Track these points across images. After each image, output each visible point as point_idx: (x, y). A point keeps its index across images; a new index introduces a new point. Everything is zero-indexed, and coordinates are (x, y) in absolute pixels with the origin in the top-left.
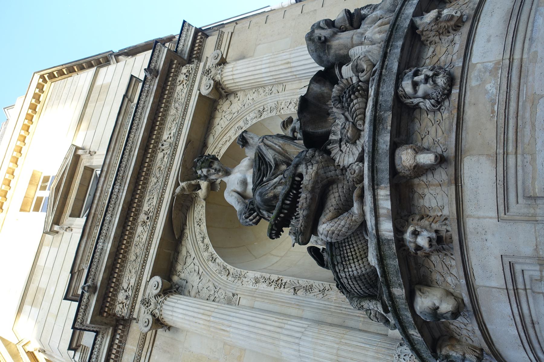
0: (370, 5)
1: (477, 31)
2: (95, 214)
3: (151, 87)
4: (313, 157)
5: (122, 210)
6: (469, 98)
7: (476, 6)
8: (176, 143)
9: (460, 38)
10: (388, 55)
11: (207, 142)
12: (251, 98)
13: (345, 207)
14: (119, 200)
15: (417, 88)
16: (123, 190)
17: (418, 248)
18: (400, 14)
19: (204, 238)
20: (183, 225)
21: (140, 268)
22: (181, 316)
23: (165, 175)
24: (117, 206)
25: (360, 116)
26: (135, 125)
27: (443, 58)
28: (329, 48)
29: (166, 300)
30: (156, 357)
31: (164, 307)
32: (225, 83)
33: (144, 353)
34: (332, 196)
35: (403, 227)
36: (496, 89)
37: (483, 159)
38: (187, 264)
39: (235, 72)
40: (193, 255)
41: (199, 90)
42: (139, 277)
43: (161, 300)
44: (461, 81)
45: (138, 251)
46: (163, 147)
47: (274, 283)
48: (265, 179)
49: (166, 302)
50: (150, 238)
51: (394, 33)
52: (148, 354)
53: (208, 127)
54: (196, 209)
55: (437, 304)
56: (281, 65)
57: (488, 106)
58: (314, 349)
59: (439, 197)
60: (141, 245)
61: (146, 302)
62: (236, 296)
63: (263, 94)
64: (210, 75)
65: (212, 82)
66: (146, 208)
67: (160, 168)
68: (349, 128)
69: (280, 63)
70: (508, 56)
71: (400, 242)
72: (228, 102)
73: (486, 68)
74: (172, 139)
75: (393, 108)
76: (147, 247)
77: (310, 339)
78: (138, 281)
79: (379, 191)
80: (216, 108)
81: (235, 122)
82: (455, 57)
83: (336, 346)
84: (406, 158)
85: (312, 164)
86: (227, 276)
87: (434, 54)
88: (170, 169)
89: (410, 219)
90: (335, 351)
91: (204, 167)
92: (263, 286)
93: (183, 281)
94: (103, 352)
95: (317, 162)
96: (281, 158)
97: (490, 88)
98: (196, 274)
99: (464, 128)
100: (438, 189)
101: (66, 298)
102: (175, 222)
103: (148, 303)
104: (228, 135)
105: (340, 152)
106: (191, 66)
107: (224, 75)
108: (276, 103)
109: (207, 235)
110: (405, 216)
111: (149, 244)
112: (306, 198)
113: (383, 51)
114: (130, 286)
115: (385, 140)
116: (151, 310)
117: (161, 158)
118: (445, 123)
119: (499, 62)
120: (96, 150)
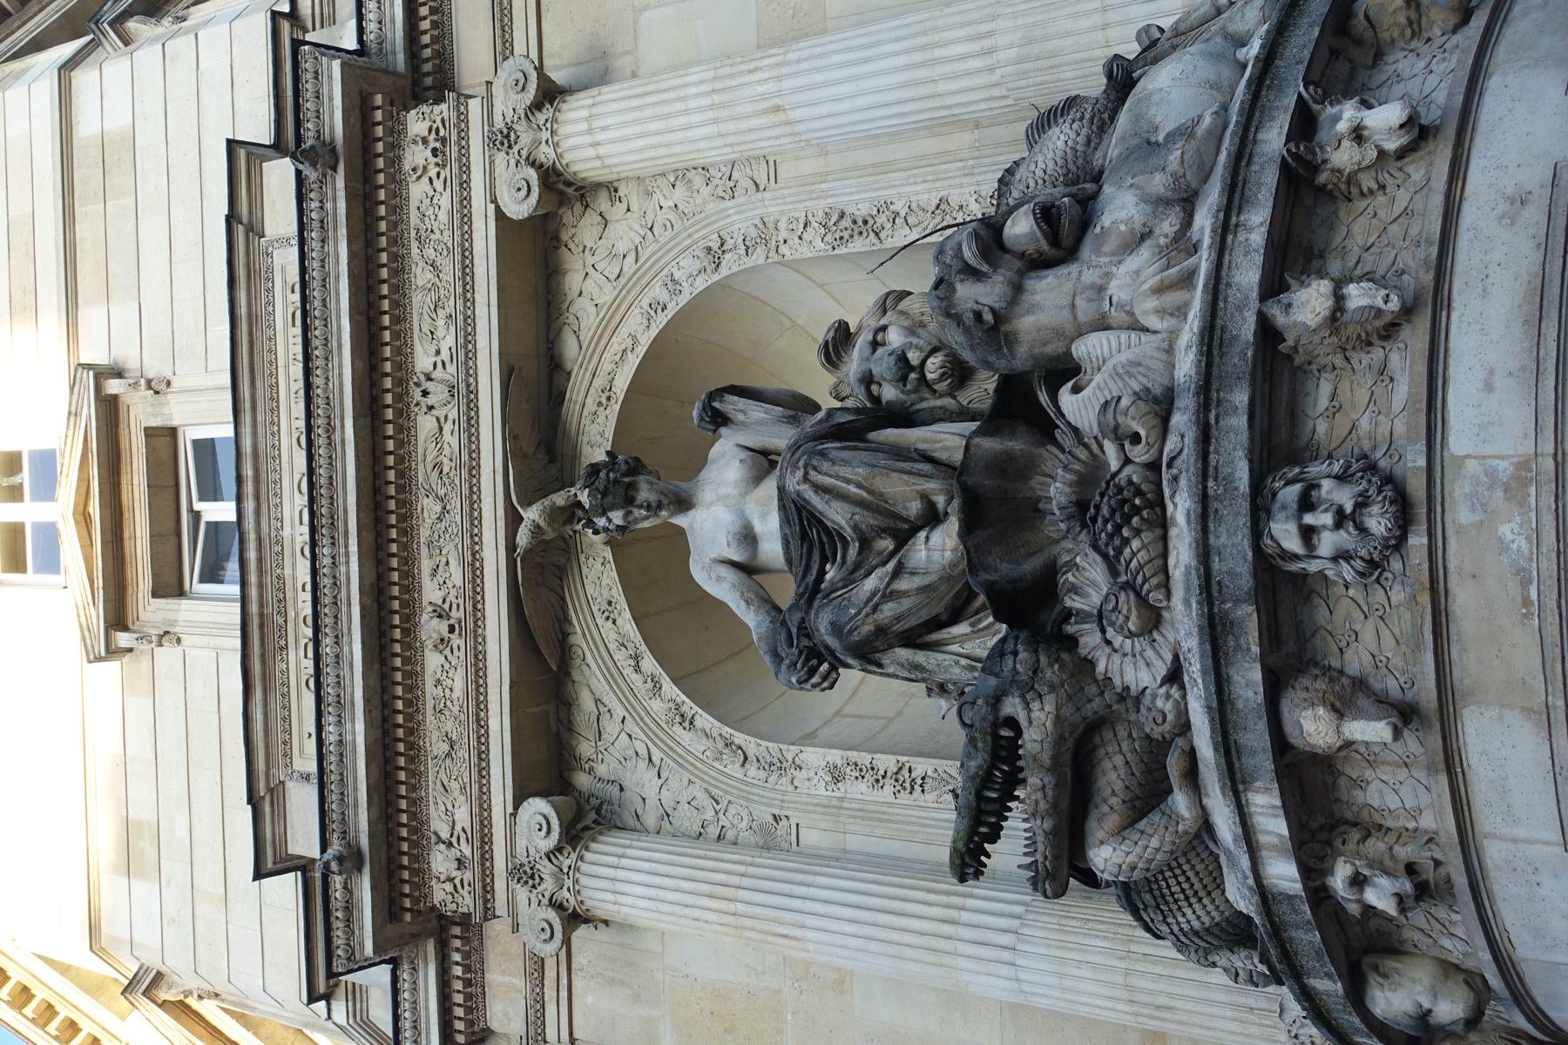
0: (1072, 102)
1: (1451, 345)
2: (261, 615)
3: (329, 205)
4: (1035, 672)
5: (363, 617)
6: (1457, 556)
7: (1434, 251)
8: (468, 385)
9: (1405, 360)
10: (1214, 432)
11: (561, 355)
12: (667, 204)
13: (1149, 796)
14: (344, 590)
15: (1315, 541)
16: (347, 554)
17: (1369, 910)
18: (1222, 287)
19: (637, 658)
20: (560, 621)
21: (475, 776)
22: (644, 903)
23: (466, 491)
24: (344, 608)
25: (1154, 581)
26: (315, 343)
27: (1365, 424)
28: (1010, 340)
29: (581, 858)
30: (590, 999)
31: (584, 880)
32: (574, 168)
33: (550, 992)
34: (1107, 765)
35: (1322, 859)
36: (1528, 539)
37: (1514, 717)
38: (608, 737)
39: (600, 137)
40: (619, 712)
41: (494, 201)
42: (475, 803)
43: (568, 862)
44: (1430, 510)
45: (450, 725)
46: (431, 400)
47: (889, 782)
48: (831, 573)
49: (584, 867)
50: (478, 686)
51: (1216, 359)
52: (564, 994)
53: (549, 305)
54: (585, 571)
55: (1426, 1005)
56: (757, 114)
57: (1513, 585)
58: (1061, 975)
59: (1405, 791)
60: (456, 709)
61: (525, 874)
62: (784, 822)
63: (706, 191)
64: (516, 149)
65: (532, 174)
66: (431, 592)
67: (438, 466)
68: (1129, 610)
69: (749, 108)
70: (1549, 447)
71: (1319, 895)
72: (591, 218)
73: (1491, 474)
74: (451, 369)
75: (1256, 594)
76: (478, 715)
77: (1042, 951)
78: (481, 815)
79: (1250, 795)
80: (558, 239)
81: (638, 288)
82: (1400, 428)
83: (1118, 963)
85: (1040, 696)
86: (743, 765)
87: (1336, 410)
88: (474, 470)
89: (1338, 842)
90: (1120, 979)
91: (613, 507)
92: (857, 789)
93: (610, 788)
94: (427, 1008)
95: (1052, 688)
96: (868, 520)
97: (1509, 537)
98: (643, 764)
99: (1454, 637)
100: (1403, 774)
101: (259, 874)
102: (538, 626)
103: (532, 877)
104: (624, 330)
105: (1108, 650)
106: (437, 109)
107: (565, 145)
108: (757, 221)
109: (644, 648)
110: (1321, 828)
111: (481, 705)
112: (1043, 788)
113: (1198, 422)
114: (458, 828)
115: (1248, 679)
116: (547, 895)
117: (432, 433)
118: (1400, 618)
119: (1527, 462)
120: (168, 374)
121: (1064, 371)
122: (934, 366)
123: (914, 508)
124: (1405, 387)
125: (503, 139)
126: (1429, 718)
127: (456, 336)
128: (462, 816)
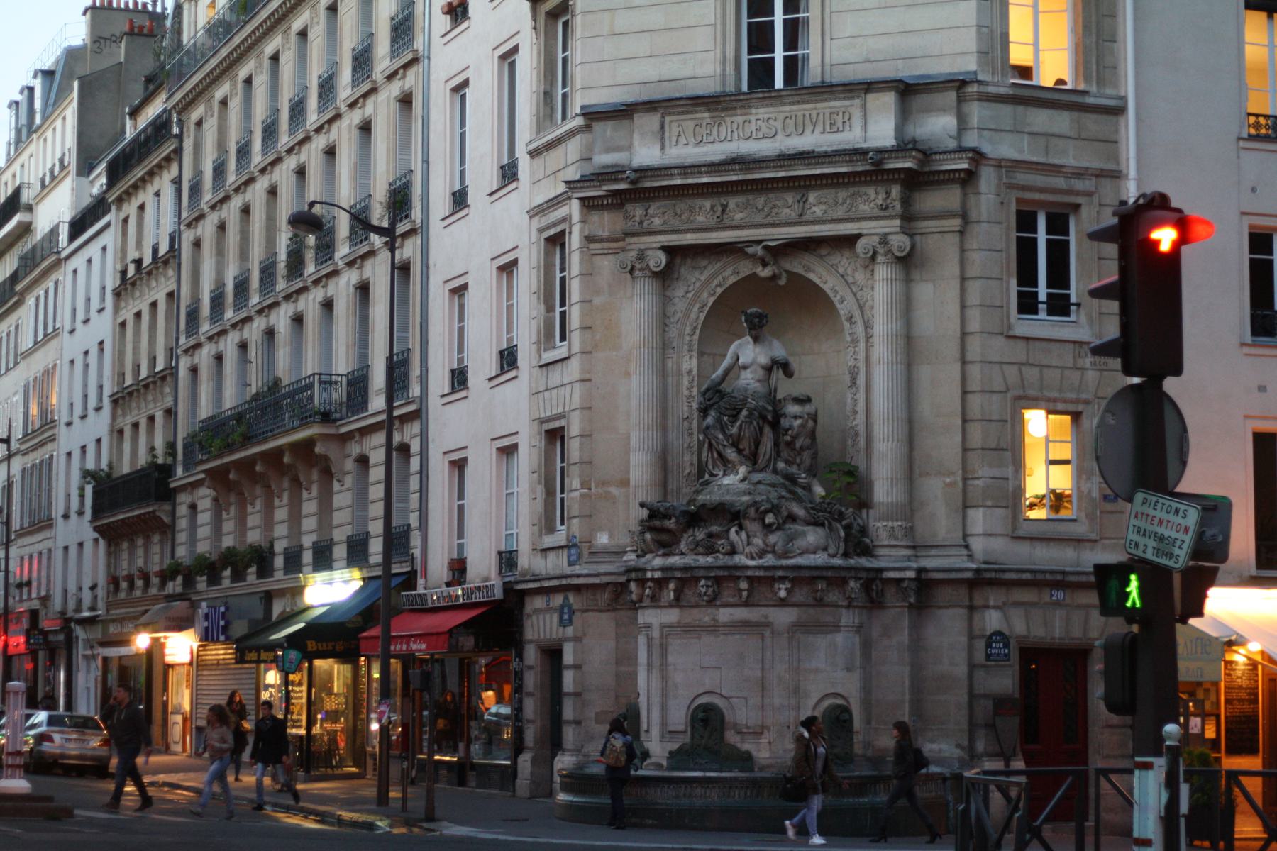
13: (662, 545)
19: (720, 285)
33: (606, 245)
48: (726, 418)
67: (775, 206)
71: (648, 580)
88: (773, 225)
92: (686, 382)
115: (678, 574)
117: (787, 205)
121: (741, 527)
122: (788, 438)
124: (731, 600)
125: (884, 239)
126: (677, 602)
127: (822, 215)
128: (657, 221)
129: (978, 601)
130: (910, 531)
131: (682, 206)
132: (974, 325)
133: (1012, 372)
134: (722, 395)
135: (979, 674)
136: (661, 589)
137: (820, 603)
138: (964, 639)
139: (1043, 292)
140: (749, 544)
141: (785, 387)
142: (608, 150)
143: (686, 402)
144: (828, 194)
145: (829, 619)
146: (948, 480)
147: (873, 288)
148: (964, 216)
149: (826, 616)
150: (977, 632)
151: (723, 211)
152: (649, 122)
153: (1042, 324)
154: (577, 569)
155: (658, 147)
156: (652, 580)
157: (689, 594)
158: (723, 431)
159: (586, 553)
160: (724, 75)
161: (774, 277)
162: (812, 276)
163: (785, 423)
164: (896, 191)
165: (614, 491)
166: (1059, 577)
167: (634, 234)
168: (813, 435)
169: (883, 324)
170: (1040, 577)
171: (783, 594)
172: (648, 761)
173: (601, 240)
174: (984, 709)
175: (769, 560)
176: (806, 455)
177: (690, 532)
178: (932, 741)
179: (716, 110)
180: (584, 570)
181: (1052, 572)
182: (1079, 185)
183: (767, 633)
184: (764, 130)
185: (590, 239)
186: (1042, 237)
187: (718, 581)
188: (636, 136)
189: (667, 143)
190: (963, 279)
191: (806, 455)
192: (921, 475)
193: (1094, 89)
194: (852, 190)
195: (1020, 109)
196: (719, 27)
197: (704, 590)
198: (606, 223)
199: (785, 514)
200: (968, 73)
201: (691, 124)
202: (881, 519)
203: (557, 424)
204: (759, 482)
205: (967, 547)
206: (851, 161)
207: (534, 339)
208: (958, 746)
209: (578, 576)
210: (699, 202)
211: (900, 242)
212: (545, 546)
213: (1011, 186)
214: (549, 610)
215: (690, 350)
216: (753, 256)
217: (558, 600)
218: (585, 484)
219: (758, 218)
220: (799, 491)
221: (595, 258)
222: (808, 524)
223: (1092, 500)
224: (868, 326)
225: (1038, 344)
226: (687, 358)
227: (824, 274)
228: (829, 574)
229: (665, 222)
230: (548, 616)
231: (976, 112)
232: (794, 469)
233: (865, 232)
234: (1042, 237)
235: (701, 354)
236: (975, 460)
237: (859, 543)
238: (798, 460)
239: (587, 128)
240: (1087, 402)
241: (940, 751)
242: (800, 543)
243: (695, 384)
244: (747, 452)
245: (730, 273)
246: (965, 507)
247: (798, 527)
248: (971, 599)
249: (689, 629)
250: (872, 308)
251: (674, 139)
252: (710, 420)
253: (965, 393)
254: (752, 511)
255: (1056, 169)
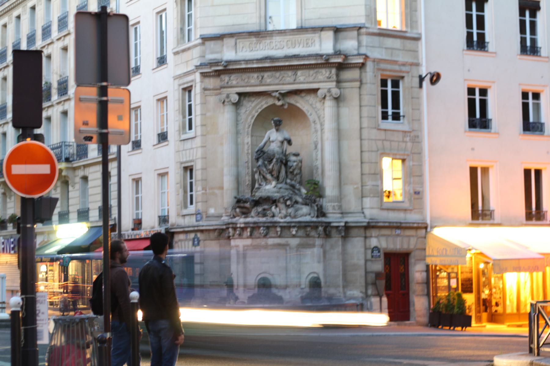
19: (260, 108)
33: (212, 91)
45: (246, 80)
71: (237, 228)
84: (249, 230)
88: (283, 84)
92: (246, 147)
115: (251, 225)
117: (289, 76)
121: (277, 206)
122: (291, 170)
123: (273, 173)
124: (273, 235)
125: (329, 91)
126: (251, 236)
128: (234, 83)
129: (368, 234)
130: (340, 207)
131: (245, 76)
132: (365, 125)
133: (379, 143)
134: (264, 153)
135: (369, 264)
136: (243, 231)
137: (308, 236)
138: (363, 250)
139: (390, 111)
140: (280, 213)
141: (290, 150)
142: (212, 53)
143: (247, 156)
144: (306, 72)
145: (311, 242)
146: (355, 186)
147: (324, 109)
148: (361, 81)
149: (310, 241)
150: (368, 247)
151: (262, 78)
152: (230, 42)
153: (390, 124)
154: (201, 223)
155: (234, 52)
156: (240, 227)
157: (256, 233)
158: (265, 166)
159: (204, 216)
160: (260, 23)
161: (283, 105)
162: (298, 105)
163: (290, 164)
164: (334, 71)
165: (216, 191)
166: (399, 225)
167: (224, 87)
168: (300, 169)
169: (329, 125)
170: (391, 224)
171: (294, 233)
172: (238, 301)
173: (209, 90)
174: (371, 277)
175: (288, 219)
176: (298, 177)
177: (255, 208)
178: (350, 290)
179: (258, 37)
180: (204, 224)
181: (396, 223)
182: (404, 69)
183: (288, 248)
184: (278, 46)
185: (205, 89)
186: (389, 89)
187: (268, 228)
188: (225, 47)
189: (238, 51)
190: (360, 106)
191: (298, 177)
192: (344, 184)
193: (409, 30)
194: (316, 70)
195: (382, 38)
196: (258, 3)
197: (262, 232)
198: (212, 83)
199: (294, 201)
200: (361, 24)
201: (248, 43)
202: (330, 201)
203: (189, 164)
204: (281, 188)
205: (363, 213)
206: (316, 59)
207: (177, 128)
208: (361, 292)
209: (203, 226)
210: (252, 75)
211: (335, 92)
212: (184, 214)
213: (379, 69)
214: (186, 240)
215: (248, 134)
216: (274, 97)
217: (192, 235)
218: (204, 189)
219: (277, 81)
220: (297, 191)
221: (207, 97)
222: (303, 204)
223: (410, 194)
224: (322, 125)
225: (389, 132)
226: (246, 138)
227: (302, 103)
228: (312, 224)
229: (238, 83)
230: (186, 243)
231: (365, 39)
232: (293, 182)
233: (321, 87)
234: (389, 89)
235: (252, 136)
236: (366, 178)
237: (321, 213)
238: (295, 179)
239: (203, 44)
240: (408, 155)
241: (354, 294)
242: (300, 212)
243: (250, 148)
244: (275, 176)
245: (265, 103)
246: (362, 197)
247: (299, 206)
248: (365, 233)
249: (256, 247)
250: (324, 117)
251: (241, 49)
252: (260, 163)
253: (362, 152)
254: (282, 200)
255: (395, 62)
